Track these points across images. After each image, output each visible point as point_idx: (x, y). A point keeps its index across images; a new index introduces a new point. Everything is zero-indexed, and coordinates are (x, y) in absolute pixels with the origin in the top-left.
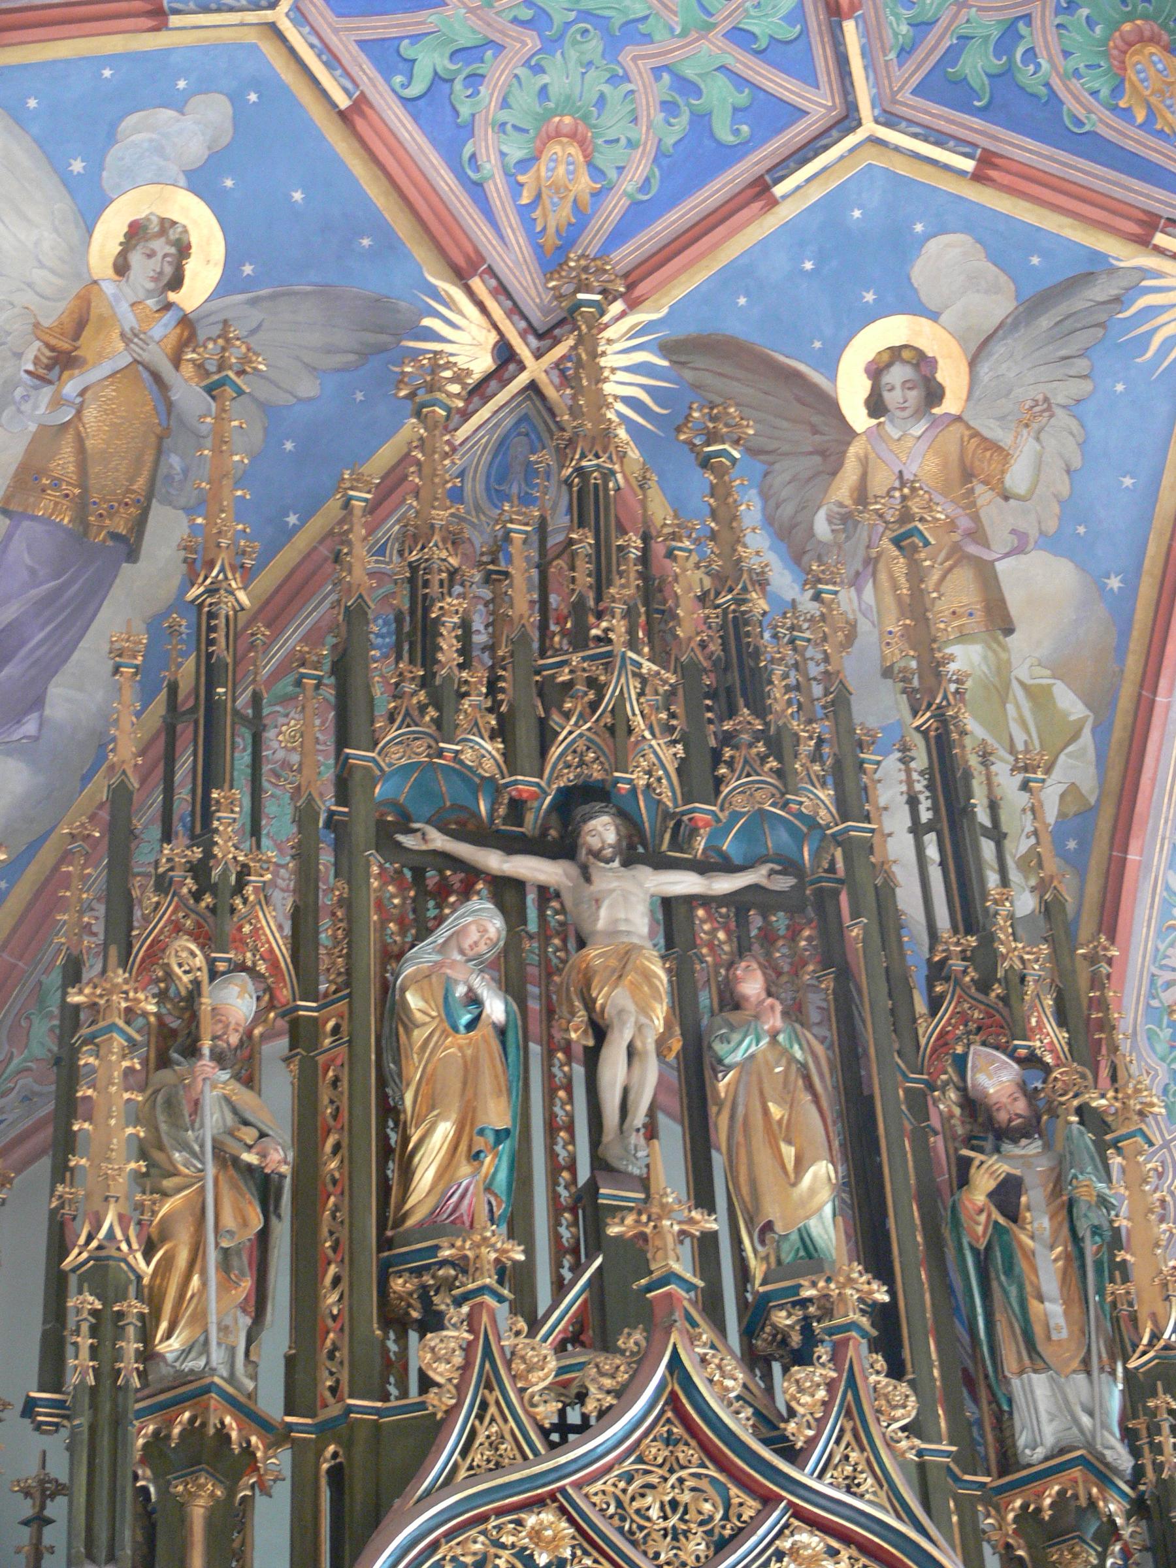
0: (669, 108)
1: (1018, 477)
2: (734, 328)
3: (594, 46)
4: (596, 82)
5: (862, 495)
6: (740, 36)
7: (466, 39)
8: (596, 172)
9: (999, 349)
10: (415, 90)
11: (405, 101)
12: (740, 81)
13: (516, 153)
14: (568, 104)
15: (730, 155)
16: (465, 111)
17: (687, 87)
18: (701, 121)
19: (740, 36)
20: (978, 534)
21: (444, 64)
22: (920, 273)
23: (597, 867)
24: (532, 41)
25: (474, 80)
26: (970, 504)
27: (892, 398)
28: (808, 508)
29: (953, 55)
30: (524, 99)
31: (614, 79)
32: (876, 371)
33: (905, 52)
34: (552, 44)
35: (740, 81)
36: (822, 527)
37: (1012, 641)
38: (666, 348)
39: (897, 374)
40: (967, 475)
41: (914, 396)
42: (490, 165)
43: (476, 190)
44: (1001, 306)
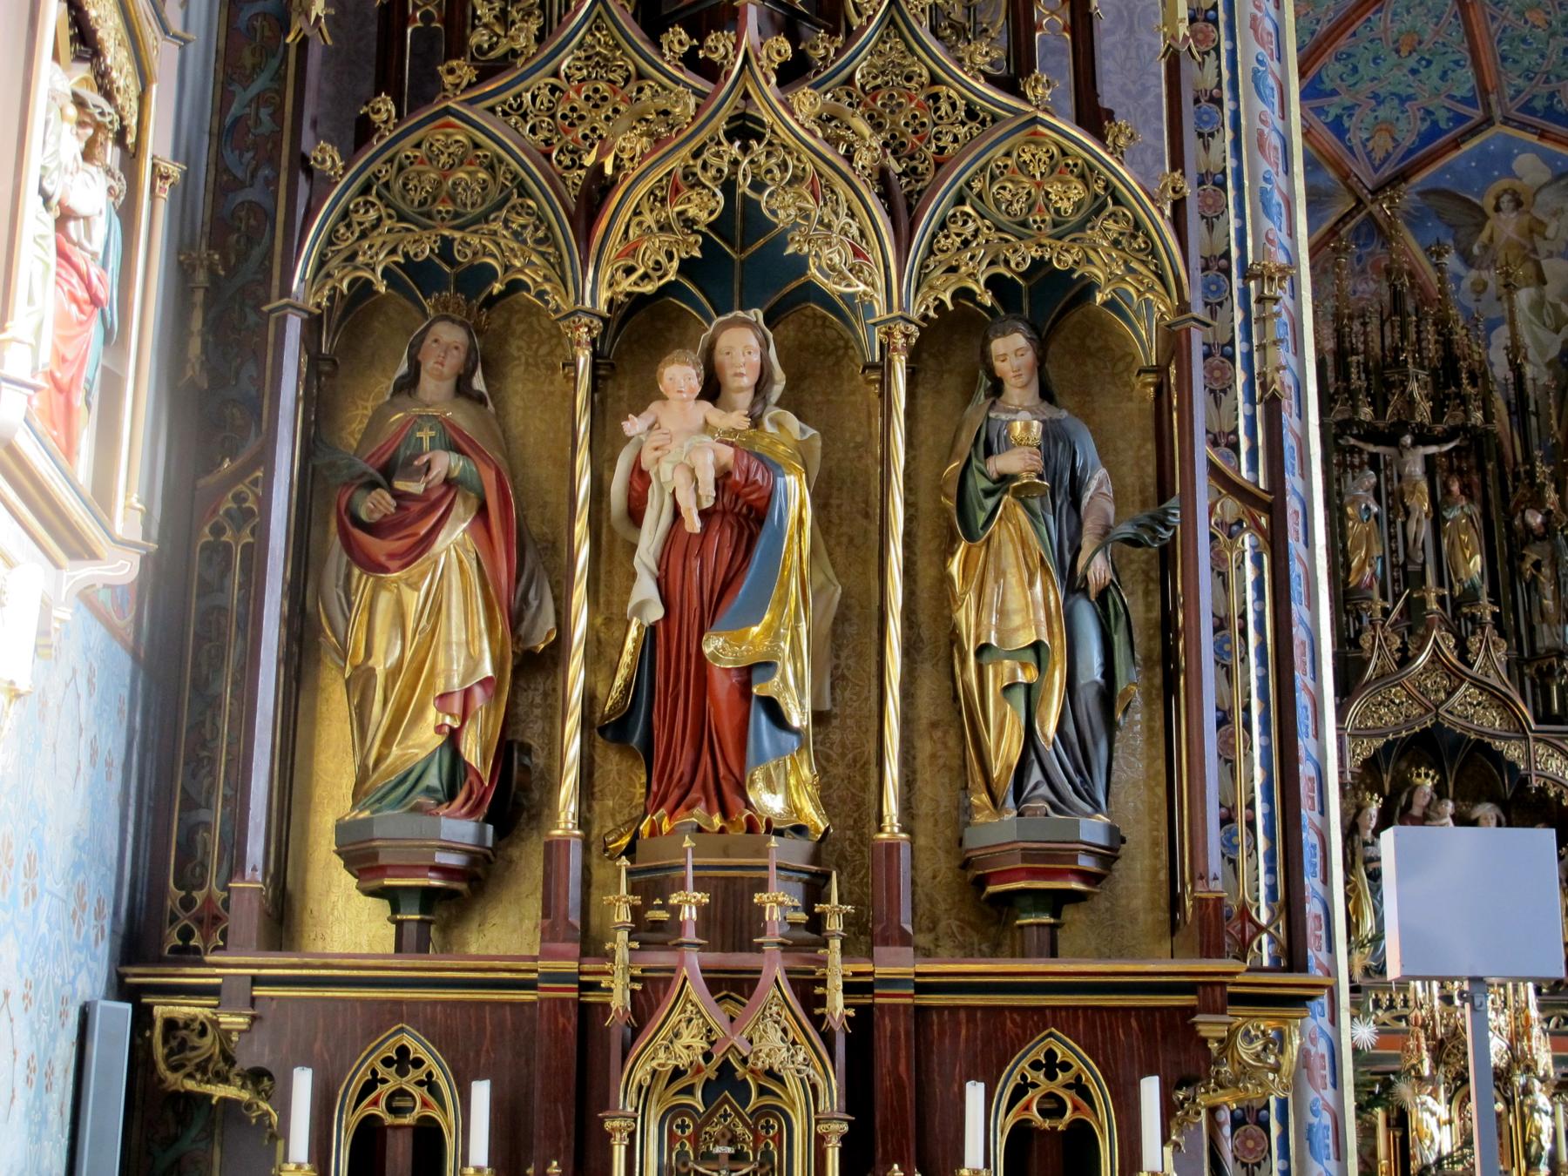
0: (1423, 120)
1: (1550, 232)
2: (1444, 185)
3: (1396, 102)
4: (1396, 113)
5: (1491, 239)
6: (1451, 97)
7: (1348, 103)
8: (1394, 139)
9: (1545, 192)
10: (1329, 120)
11: (1326, 124)
12: (1449, 110)
13: (1365, 136)
14: (1385, 121)
15: (1446, 132)
16: (1347, 125)
17: (1429, 113)
18: (1435, 123)
19: (1451, 97)
20: (1535, 250)
21: (1339, 111)
22: (1515, 165)
23: (1404, 451)
24: (1373, 102)
25: (1350, 116)
26: (1532, 241)
27: (1503, 206)
28: (1471, 244)
29: (1530, 101)
30: (1370, 119)
31: (1403, 112)
32: (1498, 198)
33: (1512, 99)
34: (1379, 104)
35: (1449, 110)
36: (1476, 250)
37: (1547, 288)
38: (1420, 194)
39: (1506, 198)
40: (1531, 231)
41: (1512, 205)
42: (1355, 142)
43: (1351, 149)
44: (1545, 176)
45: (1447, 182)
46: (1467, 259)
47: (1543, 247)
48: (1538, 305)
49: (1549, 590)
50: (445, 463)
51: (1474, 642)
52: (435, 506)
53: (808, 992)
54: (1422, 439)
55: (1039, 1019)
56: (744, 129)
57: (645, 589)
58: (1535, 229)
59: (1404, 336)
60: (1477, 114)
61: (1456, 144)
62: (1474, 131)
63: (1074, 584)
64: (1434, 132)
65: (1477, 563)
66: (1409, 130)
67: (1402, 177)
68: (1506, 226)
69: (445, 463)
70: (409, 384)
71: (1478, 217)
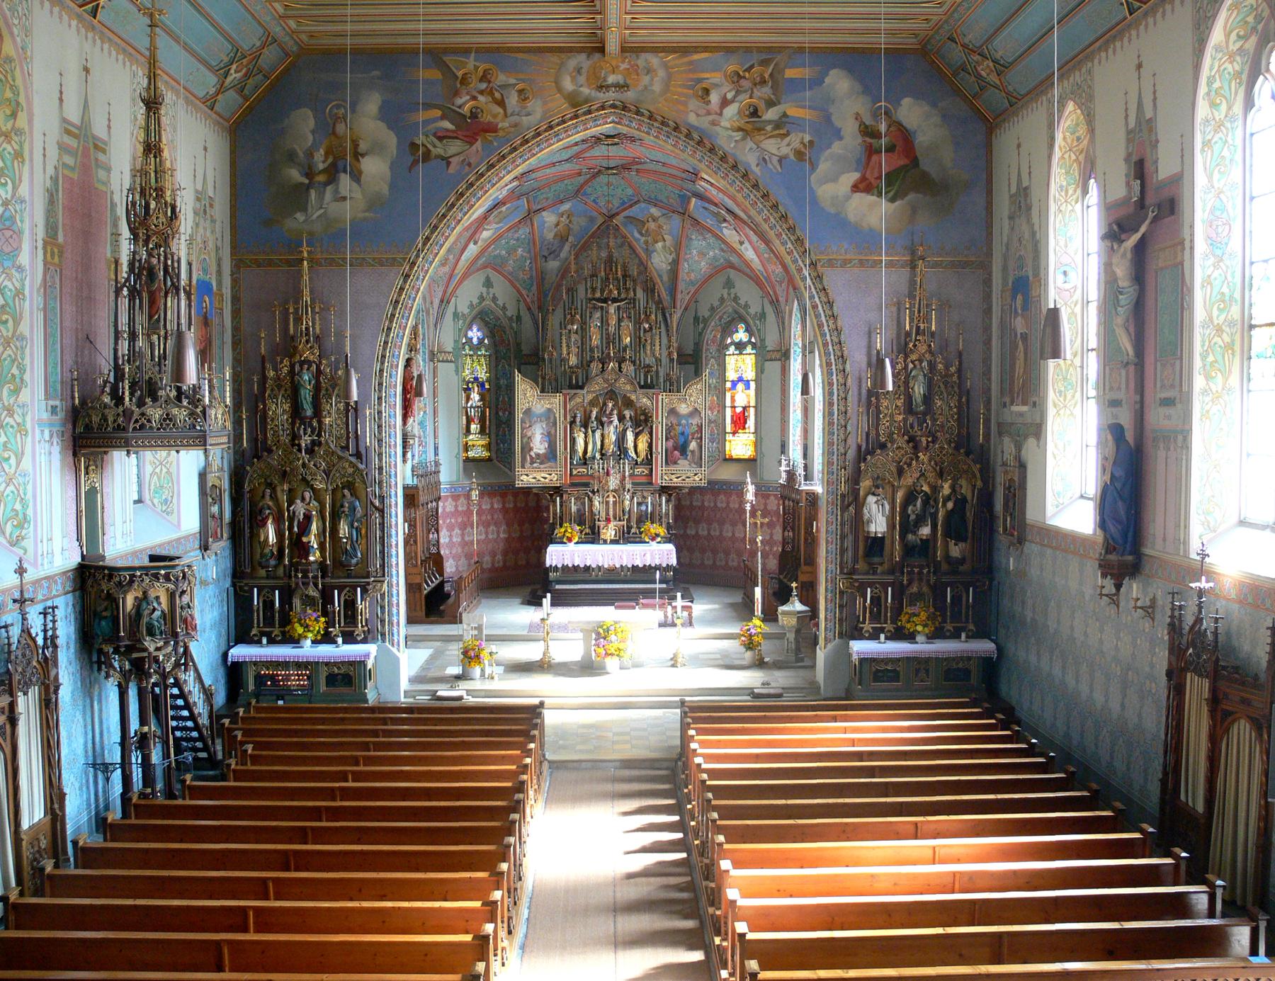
45: (631, 214)
46: (642, 235)
47: (663, 232)
48: (664, 247)
49: (649, 348)
50: (267, 512)
51: (623, 366)
52: (267, 518)
53: (316, 585)
54: (615, 300)
55: (346, 587)
56: (304, 465)
57: (296, 529)
58: (660, 227)
59: (611, 270)
60: (636, 199)
61: (631, 206)
62: (636, 203)
63: (352, 526)
64: (624, 203)
65: (629, 339)
66: (616, 203)
67: (617, 214)
68: (652, 225)
69: (267, 512)
70: (263, 497)
71: (643, 223)
